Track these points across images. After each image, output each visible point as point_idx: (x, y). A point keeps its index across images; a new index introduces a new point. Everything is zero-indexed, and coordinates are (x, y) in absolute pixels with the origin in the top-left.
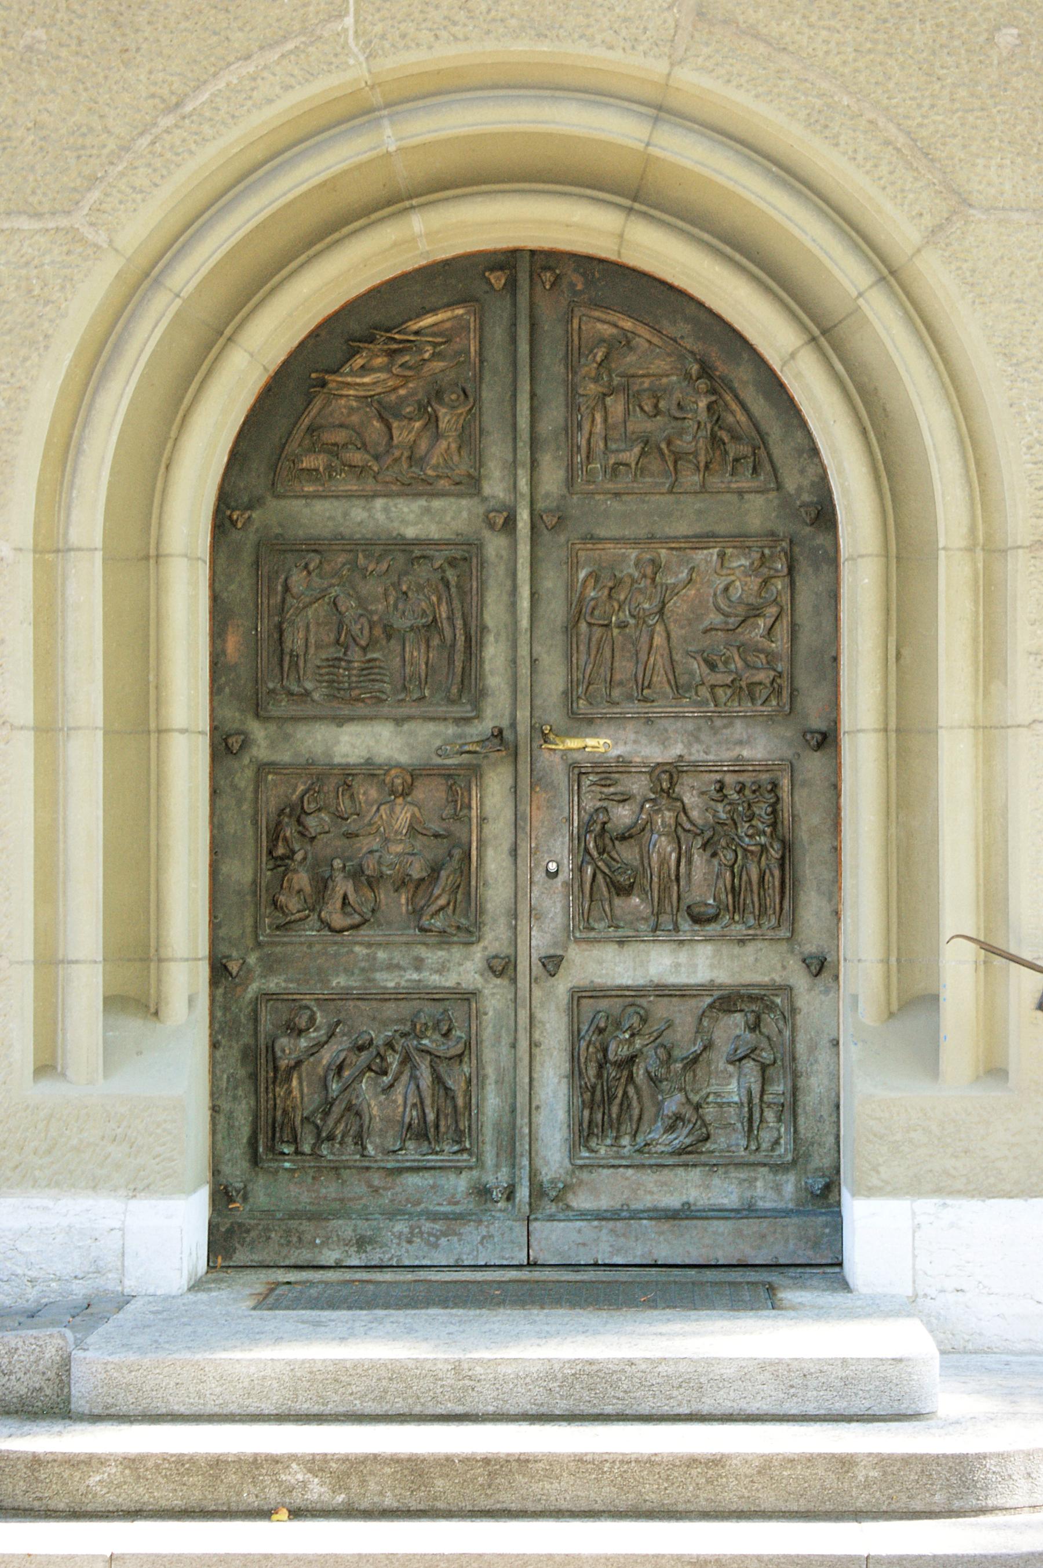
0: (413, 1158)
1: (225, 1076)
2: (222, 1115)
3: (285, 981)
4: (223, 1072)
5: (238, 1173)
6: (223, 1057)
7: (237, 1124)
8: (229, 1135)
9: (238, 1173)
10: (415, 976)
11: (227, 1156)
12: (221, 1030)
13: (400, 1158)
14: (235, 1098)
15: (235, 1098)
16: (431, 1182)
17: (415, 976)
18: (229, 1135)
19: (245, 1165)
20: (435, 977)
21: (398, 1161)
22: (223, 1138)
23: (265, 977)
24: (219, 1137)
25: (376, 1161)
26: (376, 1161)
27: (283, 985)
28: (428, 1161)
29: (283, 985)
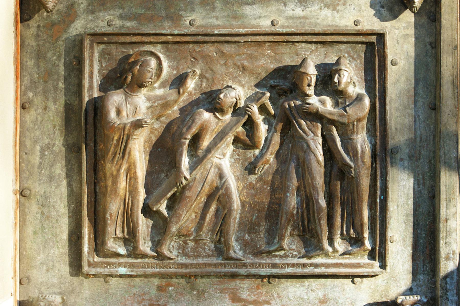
0: (295, 261)
1: (38, 148)
2: (33, 202)
3: (121, 17)
4: (36, 142)
5: (55, 281)
6: (35, 122)
7: (53, 214)
8: (43, 228)
9: (55, 281)
10: (299, 11)
11: (40, 258)
12: (33, 84)
13: (277, 261)
14: (51, 178)
15: (51, 178)
16: (321, 295)
17: (299, 11)
18: (43, 228)
19: (65, 269)
20: (326, 13)
21: (275, 266)
22: (35, 233)
23: (93, 12)
24: (30, 230)
25: (245, 265)
26: (245, 265)
27: (118, 23)
28: (316, 266)
29: (118, 23)
